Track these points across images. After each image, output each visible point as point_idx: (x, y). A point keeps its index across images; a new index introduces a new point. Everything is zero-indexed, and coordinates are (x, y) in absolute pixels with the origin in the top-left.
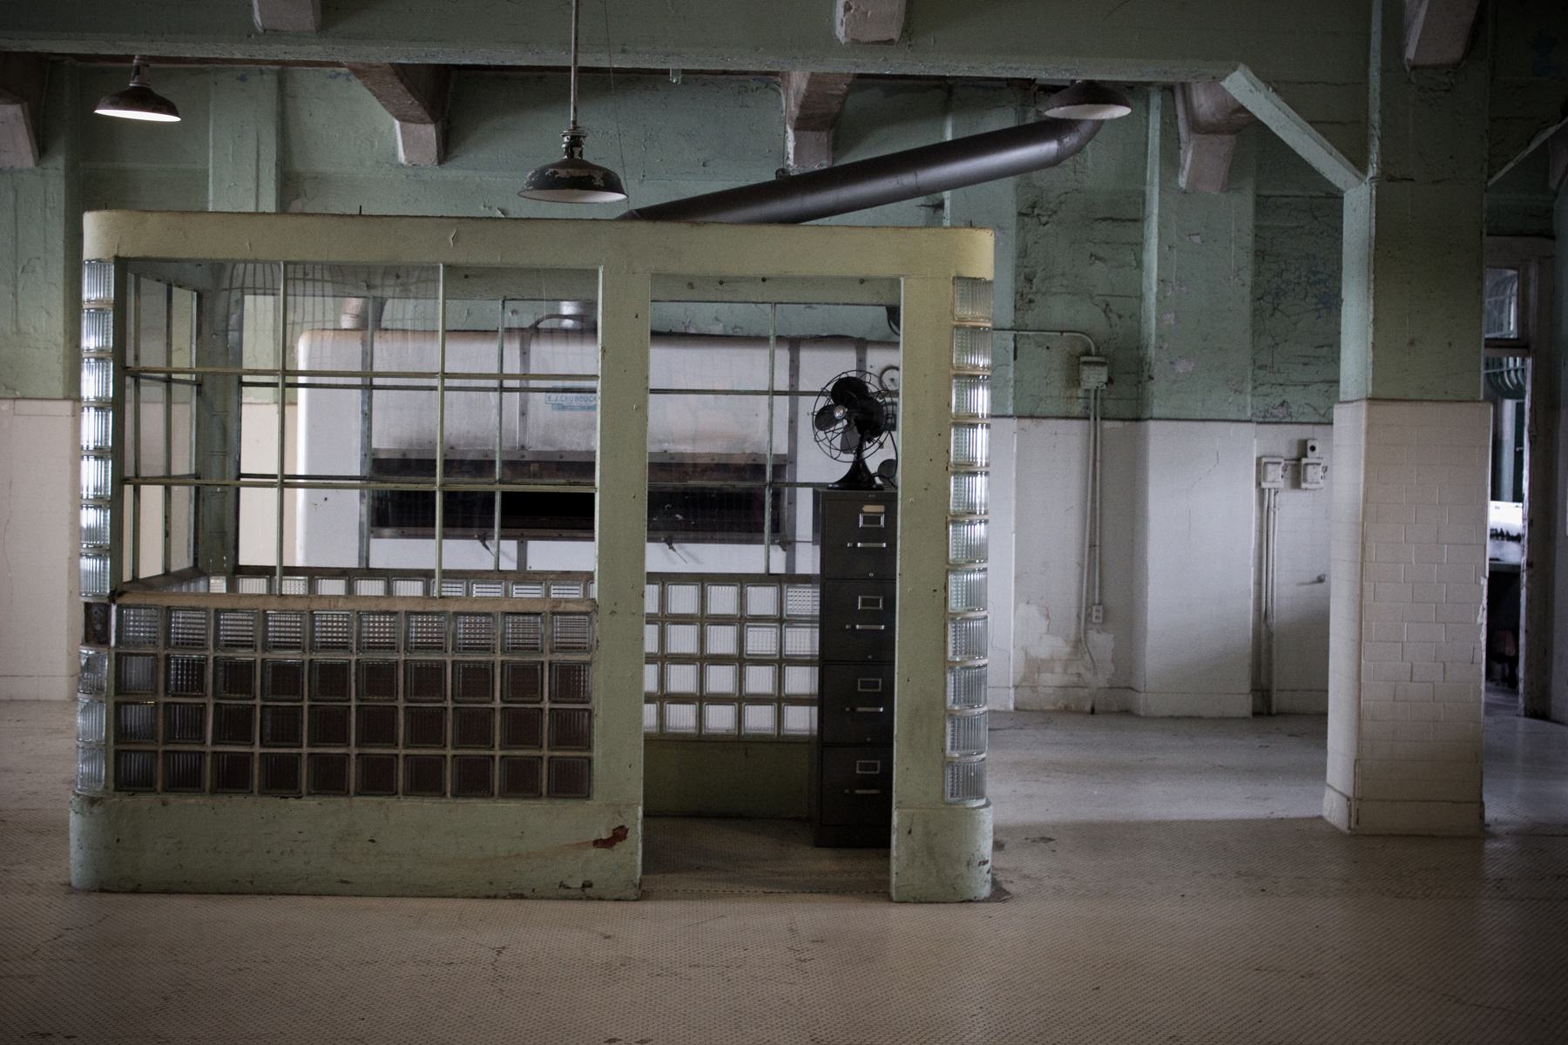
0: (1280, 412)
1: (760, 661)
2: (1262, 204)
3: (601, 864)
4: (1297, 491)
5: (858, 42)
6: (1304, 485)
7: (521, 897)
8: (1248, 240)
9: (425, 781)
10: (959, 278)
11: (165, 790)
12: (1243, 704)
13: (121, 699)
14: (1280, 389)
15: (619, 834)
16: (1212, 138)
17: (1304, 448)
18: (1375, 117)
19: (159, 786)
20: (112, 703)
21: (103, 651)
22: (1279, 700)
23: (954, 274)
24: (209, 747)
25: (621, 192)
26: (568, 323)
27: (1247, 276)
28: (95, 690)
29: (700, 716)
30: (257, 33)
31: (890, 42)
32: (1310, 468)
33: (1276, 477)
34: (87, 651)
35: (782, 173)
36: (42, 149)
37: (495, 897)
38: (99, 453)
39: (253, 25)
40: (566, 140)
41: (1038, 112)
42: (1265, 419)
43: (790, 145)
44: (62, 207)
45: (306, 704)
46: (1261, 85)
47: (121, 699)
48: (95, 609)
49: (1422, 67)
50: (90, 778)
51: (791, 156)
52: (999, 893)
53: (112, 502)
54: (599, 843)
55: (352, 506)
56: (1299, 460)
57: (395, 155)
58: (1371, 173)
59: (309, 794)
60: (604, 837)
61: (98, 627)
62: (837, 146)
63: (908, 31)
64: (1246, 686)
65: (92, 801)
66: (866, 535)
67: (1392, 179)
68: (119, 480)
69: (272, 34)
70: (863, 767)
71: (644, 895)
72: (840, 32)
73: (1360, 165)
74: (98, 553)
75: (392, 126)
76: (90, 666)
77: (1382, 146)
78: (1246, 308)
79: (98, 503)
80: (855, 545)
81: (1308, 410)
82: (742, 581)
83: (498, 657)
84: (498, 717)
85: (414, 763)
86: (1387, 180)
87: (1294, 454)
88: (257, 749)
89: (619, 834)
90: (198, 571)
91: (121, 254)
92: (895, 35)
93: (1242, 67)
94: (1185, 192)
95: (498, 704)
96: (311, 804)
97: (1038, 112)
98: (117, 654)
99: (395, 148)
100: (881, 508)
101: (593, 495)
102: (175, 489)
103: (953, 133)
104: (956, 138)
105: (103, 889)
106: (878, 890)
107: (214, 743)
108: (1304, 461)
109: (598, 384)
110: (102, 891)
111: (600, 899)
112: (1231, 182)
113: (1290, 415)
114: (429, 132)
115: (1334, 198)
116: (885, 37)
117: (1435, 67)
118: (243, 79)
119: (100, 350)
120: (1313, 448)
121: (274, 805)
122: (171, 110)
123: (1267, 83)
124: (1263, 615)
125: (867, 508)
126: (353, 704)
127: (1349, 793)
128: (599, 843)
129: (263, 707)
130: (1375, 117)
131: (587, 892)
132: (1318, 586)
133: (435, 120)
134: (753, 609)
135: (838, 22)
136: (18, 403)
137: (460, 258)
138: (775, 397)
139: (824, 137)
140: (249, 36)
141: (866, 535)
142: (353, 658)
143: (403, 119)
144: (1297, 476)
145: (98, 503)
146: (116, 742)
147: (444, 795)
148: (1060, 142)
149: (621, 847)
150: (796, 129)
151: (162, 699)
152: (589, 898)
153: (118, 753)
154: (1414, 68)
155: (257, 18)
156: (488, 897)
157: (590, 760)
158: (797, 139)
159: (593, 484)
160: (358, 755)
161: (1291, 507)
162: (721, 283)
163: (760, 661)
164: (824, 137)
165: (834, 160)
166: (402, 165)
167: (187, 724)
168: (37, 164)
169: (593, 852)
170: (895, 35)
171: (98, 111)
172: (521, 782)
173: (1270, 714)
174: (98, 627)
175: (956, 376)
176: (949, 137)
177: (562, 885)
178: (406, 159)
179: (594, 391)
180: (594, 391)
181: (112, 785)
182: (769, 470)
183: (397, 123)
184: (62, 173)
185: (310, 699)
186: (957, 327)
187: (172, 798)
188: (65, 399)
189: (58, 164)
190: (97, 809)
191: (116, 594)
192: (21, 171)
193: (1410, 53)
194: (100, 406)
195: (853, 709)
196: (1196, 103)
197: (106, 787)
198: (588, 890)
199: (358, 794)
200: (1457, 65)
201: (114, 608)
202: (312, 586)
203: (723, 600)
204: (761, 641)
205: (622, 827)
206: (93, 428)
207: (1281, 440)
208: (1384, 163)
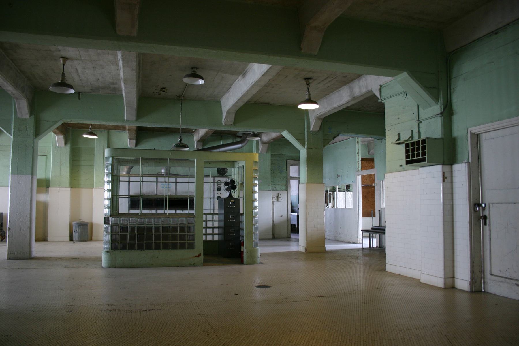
0: (275, 189)
1: (210, 228)
2: (272, 155)
3: (196, 260)
4: (278, 202)
5: (227, 125)
6: (279, 201)
7: (183, 266)
8: (270, 161)
9: (166, 247)
10: (254, 161)
11: (120, 249)
12: (271, 237)
13: (112, 234)
14: (274, 185)
15: (200, 255)
16: (265, 144)
17: (279, 195)
18: (306, 139)
19: (119, 248)
20: (111, 235)
21: (109, 225)
22: (276, 236)
23: (253, 160)
24: (128, 242)
27: (270, 167)
28: (107, 232)
30: (125, 121)
31: (231, 125)
32: (280, 198)
33: (275, 199)
34: (105, 226)
36: (66, 143)
37: (179, 267)
39: (124, 119)
40: (179, 139)
41: (236, 140)
42: (273, 190)
43: (196, 145)
44: (69, 153)
45: (145, 234)
46: (289, 133)
47: (112, 234)
48: (106, 218)
49: (313, 131)
50: (107, 248)
51: (196, 146)
52: (261, 263)
54: (196, 257)
56: (278, 197)
57: (128, 145)
58: (306, 147)
59: (146, 250)
60: (197, 255)
61: (107, 221)
62: (204, 145)
63: (234, 123)
64: (271, 233)
65: (107, 252)
66: (231, 205)
67: (309, 148)
69: (128, 121)
70: (231, 244)
71: (204, 265)
72: (223, 123)
73: (304, 146)
75: (128, 140)
76: (107, 228)
77: (307, 143)
78: (270, 172)
80: (230, 207)
81: (279, 189)
83: (179, 225)
84: (178, 236)
85: (164, 244)
86: (308, 148)
87: (277, 196)
88: (137, 242)
89: (200, 255)
91: (113, 156)
92: (232, 124)
93: (286, 130)
94: (260, 153)
95: (178, 233)
96: (146, 252)
97: (236, 140)
100: (233, 201)
103: (223, 143)
104: (223, 144)
105: (109, 267)
106: (242, 262)
107: (129, 241)
108: (279, 197)
110: (109, 268)
111: (196, 266)
112: (267, 152)
113: (276, 189)
114: (134, 141)
115: (298, 151)
116: (230, 124)
117: (315, 131)
118: (101, 132)
120: (280, 195)
121: (139, 252)
122: (96, 135)
123: (290, 133)
124: (273, 222)
125: (231, 201)
126: (153, 234)
127: (305, 246)
128: (196, 257)
129: (137, 235)
130: (306, 139)
131: (195, 265)
132: (281, 217)
135: (223, 121)
136: (61, 188)
137: (172, 157)
139: (201, 143)
140: (124, 121)
141: (231, 205)
142: (153, 226)
144: (278, 199)
147: (169, 249)
148: (242, 144)
149: (200, 257)
150: (197, 142)
151: (120, 233)
152: (195, 266)
154: (312, 131)
155: (125, 118)
156: (178, 267)
157: (194, 242)
158: (197, 143)
160: (154, 243)
161: (277, 204)
163: (210, 228)
164: (201, 143)
165: (203, 147)
167: (124, 238)
168: (65, 146)
170: (232, 124)
171: (84, 136)
172: (182, 247)
173: (275, 238)
174: (107, 221)
175: (254, 177)
176: (221, 144)
177: (190, 264)
178: (130, 146)
184: (69, 147)
185: (146, 233)
186: (254, 169)
187: (121, 251)
188: (69, 187)
189: (69, 146)
190: (108, 253)
191: (111, 216)
192: (62, 147)
193: (311, 129)
195: (230, 235)
196: (263, 139)
198: (195, 265)
199: (154, 249)
200: (318, 131)
207: (275, 193)
208: (308, 146)
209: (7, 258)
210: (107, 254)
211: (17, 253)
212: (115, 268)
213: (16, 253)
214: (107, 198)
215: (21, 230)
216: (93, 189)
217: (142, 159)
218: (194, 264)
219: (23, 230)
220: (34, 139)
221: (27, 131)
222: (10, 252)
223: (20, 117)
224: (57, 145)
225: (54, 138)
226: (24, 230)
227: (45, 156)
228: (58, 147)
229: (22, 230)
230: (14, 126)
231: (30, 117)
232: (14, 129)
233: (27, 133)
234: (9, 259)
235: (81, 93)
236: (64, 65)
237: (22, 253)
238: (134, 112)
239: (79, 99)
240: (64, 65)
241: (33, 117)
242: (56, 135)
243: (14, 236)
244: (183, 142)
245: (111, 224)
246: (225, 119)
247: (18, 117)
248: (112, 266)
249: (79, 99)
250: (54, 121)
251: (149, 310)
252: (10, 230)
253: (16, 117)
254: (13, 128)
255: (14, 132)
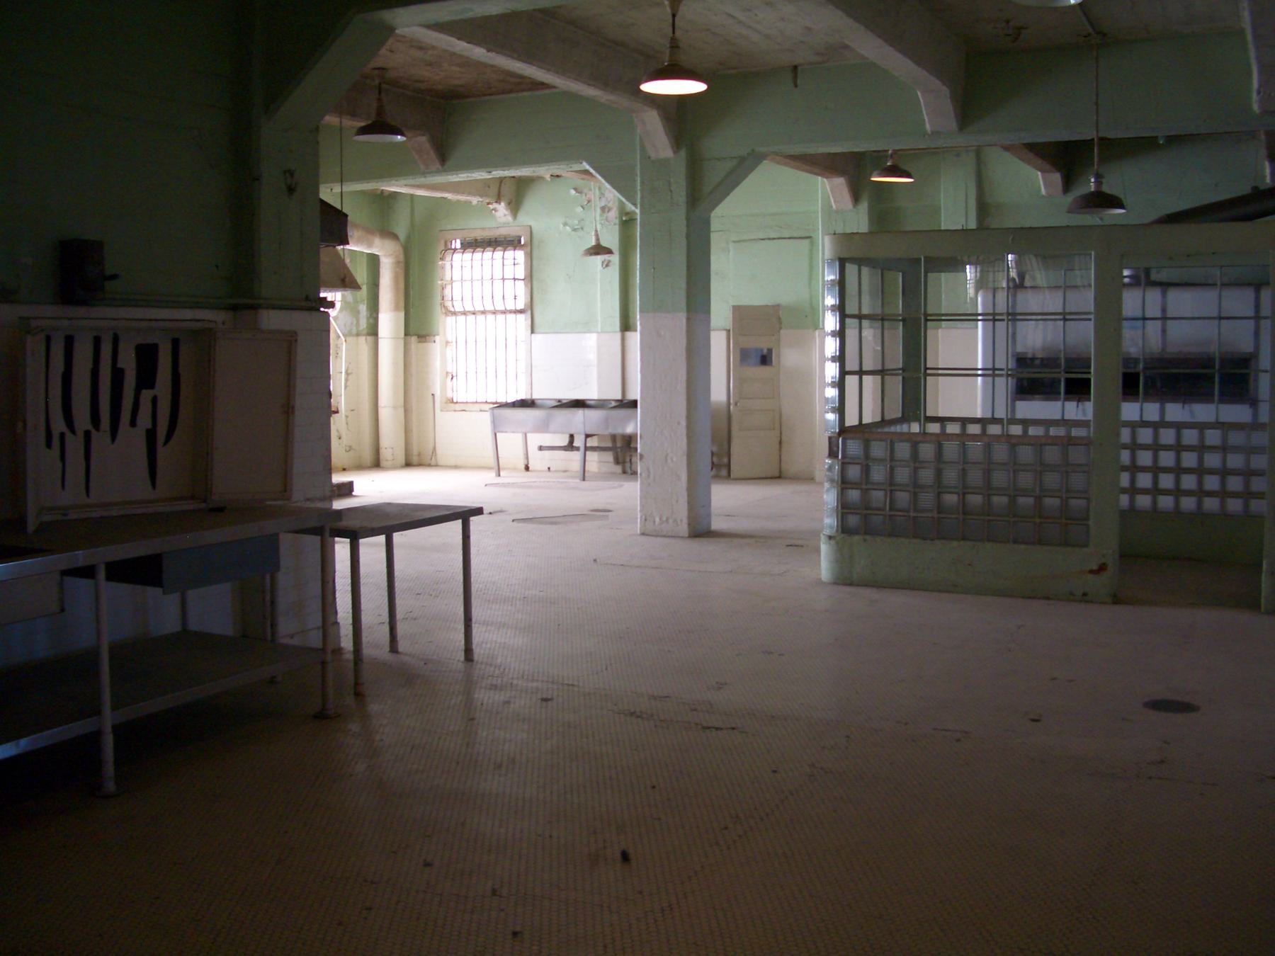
1: (1211, 472)
13: (844, 486)
21: (836, 461)
25: (1122, 207)
26: (1126, 280)
29: (1177, 502)
35: (1255, 188)
36: (856, 198)
38: (833, 359)
43: (1268, 171)
53: (840, 385)
54: (1091, 572)
55: (1004, 386)
57: (1040, 190)
65: (830, 537)
68: (843, 373)
69: (936, 133)
72: (1256, 107)
74: (833, 410)
75: (1038, 175)
79: (833, 385)
82: (1201, 427)
89: (1102, 568)
90: (904, 419)
91: (842, 257)
98: (843, 463)
99: (1039, 187)
101: (1090, 379)
102: (864, 377)
109: (1092, 317)
111: (1092, 602)
114: (1057, 177)
119: (832, 306)
122: (909, 176)
128: (1091, 572)
131: (1085, 598)
133: (1059, 170)
134: (1208, 442)
138: (1222, 321)
143: (1043, 171)
145: (833, 385)
146: (843, 508)
152: (1087, 602)
153: (842, 513)
155: (928, 127)
156: (1030, 598)
159: (1090, 373)
162: (1188, 256)
166: (1043, 196)
169: (1090, 576)
179: (1090, 320)
180: (1090, 320)
181: (840, 530)
182: (1217, 362)
183: (1039, 173)
189: (864, 206)
190: (832, 542)
194: (833, 334)
197: (837, 531)
201: (840, 439)
202: (964, 428)
203: (1190, 437)
204: (1212, 460)
205: (1104, 564)
206: (831, 346)
209: (639, 532)
210: (830, 544)
211: (660, 519)
212: (851, 584)
213: (657, 519)
214: (832, 382)
215: (666, 460)
216: (940, 331)
217: (925, 258)
218: (1085, 594)
219: (672, 461)
220: (688, 212)
221: (671, 191)
222: (644, 517)
223: (653, 156)
224: (832, 207)
225: (823, 183)
226: (674, 459)
227: (807, 241)
228: (837, 212)
229: (669, 461)
230: (642, 183)
231: (675, 152)
232: (642, 190)
233: (672, 198)
234: (643, 534)
235: (799, 68)
236: (674, 16)
237: (671, 521)
238: (948, 107)
239: (796, 86)
240: (674, 16)
241: (683, 153)
242: (825, 180)
243: (652, 476)
244: (1106, 189)
245: (840, 457)
246: (1259, 92)
247: (649, 158)
248: (845, 578)
249: (796, 86)
250: (735, 158)
251: (717, 729)
252: (644, 460)
253: (645, 157)
254: (639, 188)
255: (642, 198)
